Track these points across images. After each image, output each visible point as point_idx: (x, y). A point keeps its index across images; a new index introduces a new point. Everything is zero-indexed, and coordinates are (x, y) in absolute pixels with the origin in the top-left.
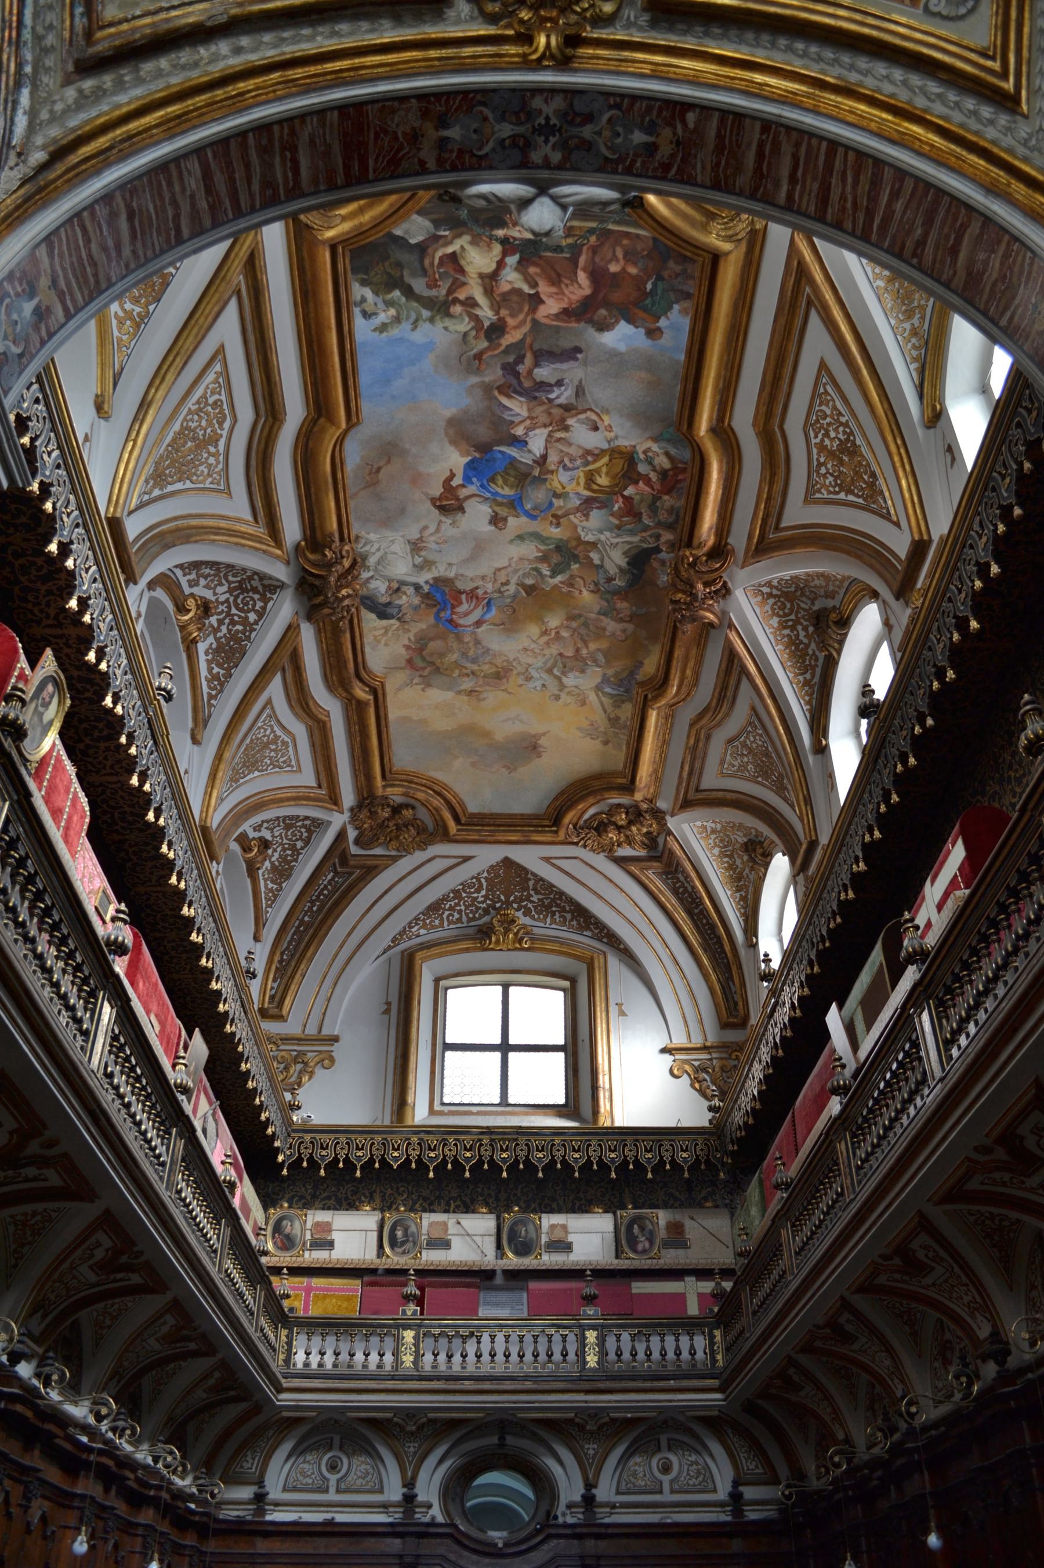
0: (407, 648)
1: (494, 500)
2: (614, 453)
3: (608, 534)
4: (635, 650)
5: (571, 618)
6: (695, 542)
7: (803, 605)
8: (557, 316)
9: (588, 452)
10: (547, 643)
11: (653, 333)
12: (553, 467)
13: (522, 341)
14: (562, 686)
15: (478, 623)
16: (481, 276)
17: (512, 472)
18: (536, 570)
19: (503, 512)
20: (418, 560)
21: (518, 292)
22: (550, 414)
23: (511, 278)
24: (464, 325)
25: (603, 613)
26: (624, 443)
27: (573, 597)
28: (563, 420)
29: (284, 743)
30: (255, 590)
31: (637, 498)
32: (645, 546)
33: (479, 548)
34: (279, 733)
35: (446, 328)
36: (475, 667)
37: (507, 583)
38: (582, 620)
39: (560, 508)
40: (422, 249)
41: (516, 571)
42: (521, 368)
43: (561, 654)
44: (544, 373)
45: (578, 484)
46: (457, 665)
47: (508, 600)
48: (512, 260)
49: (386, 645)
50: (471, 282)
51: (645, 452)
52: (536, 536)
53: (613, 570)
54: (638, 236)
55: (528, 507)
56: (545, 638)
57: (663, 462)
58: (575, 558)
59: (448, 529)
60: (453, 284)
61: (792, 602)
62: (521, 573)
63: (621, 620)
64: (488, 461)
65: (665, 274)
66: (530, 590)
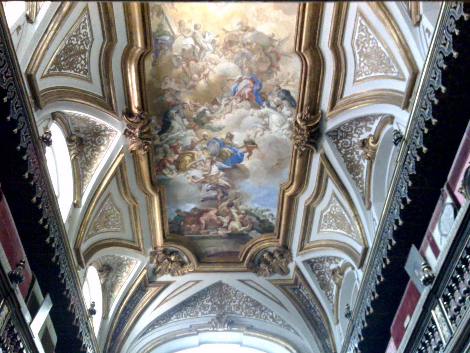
0: (278, 69)
1: (232, 146)
2: (185, 170)
3: (182, 135)
4: (158, 75)
5: (193, 87)
6: (146, 156)
7: (89, 135)
8: (210, 210)
9: (195, 168)
10: (204, 69)
11: (178, 211)
12: (208, 160)
13: (221, 204)
14: (194, 37)
15: (240, 80)
16: (235, 220)
17: (224, 158)
18: (212, 113)
19: (228, 141)
20: (266, 119)
21: (223, 216)
22: (211, 180)
23: (225, 220)
24: (241, 207)
25: (177, 92)
26: (182, 175)
27: (194, 99)
28: (206, 178)
29: (358, 46)
30: (342, 131)
31: (173, 154)
32: (165, 134)
33: (238, 123)
34: (358, 56)
35: (247, 206)
36: (243, 50)
37: (226, 105)
38: (188, 86)
39: (204, 144)
40: (253, 229)
41: (222, 112)
42: (221, 194)
43: (196, 61)
44: (213, 194)
45: (197, 155)
46: (253, 52)
47: (225, 95)
48: (225, 225)
49: (289, 74)
50: (238, 219)
51: (173, 174)
52: (213, 130)
53: (177, 117)
54: (188, 234)
55: (217, 143)
56: (206, 72)
57: (165, 171)
58: (195, 120)
59: (251, 133)
60: (243, 219)
61: (94, 133)
62: (219, 111)
63: (168, 90)
64: (234, 162)
65: (177, 227)
66: (215, 102)
